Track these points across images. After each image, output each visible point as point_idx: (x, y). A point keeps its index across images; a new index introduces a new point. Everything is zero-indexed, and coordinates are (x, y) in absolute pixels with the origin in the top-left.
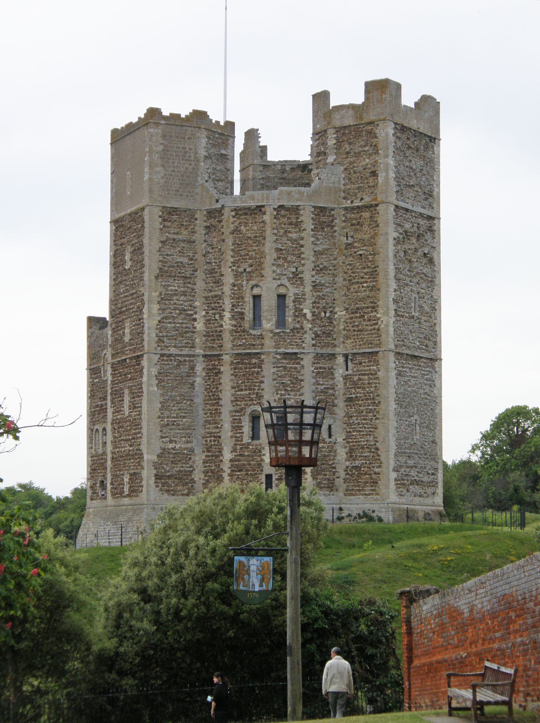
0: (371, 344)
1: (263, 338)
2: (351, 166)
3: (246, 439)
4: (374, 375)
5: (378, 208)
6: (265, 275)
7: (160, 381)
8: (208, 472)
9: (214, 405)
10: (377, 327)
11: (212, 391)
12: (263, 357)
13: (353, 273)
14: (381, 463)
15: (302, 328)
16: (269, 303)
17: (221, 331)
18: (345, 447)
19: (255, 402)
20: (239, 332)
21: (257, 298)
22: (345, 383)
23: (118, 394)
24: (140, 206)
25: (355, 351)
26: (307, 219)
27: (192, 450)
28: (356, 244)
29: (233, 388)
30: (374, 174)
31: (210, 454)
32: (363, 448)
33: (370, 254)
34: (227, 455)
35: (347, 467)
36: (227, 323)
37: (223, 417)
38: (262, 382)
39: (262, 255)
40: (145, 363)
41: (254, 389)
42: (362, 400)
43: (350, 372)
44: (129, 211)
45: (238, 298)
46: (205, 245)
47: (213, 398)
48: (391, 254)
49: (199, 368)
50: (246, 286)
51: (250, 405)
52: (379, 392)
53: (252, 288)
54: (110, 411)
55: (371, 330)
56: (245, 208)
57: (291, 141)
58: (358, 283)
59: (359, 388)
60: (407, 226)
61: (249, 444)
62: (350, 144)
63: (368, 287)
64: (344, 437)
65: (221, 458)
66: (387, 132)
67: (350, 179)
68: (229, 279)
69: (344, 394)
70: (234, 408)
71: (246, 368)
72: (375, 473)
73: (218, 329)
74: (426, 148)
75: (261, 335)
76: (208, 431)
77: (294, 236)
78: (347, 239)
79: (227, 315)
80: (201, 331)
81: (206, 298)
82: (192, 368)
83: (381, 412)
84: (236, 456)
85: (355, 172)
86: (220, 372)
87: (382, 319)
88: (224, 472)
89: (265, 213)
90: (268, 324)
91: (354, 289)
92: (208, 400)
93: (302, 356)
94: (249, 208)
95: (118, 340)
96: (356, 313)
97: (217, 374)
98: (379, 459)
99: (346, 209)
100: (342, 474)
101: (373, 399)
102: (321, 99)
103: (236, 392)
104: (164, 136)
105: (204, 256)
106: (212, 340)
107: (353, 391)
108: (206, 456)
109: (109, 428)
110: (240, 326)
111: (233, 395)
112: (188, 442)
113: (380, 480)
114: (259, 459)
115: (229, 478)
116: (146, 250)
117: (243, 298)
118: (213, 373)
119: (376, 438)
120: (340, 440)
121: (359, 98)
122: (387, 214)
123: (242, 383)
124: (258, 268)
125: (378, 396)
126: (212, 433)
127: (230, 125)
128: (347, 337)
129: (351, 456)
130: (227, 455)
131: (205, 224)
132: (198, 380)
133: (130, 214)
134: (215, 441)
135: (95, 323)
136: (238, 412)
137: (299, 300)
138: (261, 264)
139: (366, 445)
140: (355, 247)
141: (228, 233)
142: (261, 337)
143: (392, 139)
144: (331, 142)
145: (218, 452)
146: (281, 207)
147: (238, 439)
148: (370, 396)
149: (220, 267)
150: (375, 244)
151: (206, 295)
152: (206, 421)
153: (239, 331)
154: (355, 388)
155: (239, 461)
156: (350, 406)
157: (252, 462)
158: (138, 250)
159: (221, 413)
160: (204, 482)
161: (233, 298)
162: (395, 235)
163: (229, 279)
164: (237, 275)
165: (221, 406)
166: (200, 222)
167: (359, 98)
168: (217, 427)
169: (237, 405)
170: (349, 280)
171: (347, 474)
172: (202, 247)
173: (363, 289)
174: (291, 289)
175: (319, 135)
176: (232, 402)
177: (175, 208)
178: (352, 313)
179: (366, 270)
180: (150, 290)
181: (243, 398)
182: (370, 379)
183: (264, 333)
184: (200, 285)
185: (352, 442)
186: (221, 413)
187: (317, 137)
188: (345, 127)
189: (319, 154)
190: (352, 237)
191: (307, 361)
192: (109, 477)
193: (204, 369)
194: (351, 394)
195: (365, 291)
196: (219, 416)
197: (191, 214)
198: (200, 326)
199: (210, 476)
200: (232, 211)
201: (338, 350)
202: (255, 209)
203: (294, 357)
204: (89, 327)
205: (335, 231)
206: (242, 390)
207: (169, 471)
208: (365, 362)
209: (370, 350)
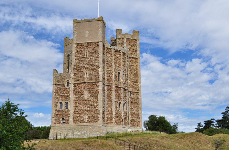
3: (118, 110)
12: (121, 88)
21: (119, 73)
24: (97, 41)
34: (114, 113)
37: (113, 102)
44: (87, 42)
45: (116, 72)
47: (110, 97)
58: (132, 75)
65: (112, 114)
68: (114, 67)
72: (139, 122)
81: (107, 70)
89: (121, 53)
97: (110, 91)
99: (129, 57)
111: (115, 97)
118: (110, 91)
128: (130, 88)
131: (107, 51)
133: (88, 43)
144: (125, 41)
147: (116, 109)
152: (107, 103)
163: (114, 67)
188: (129, 39)
191: (127, 92)
198: (106, 78)
200: (114, 50)
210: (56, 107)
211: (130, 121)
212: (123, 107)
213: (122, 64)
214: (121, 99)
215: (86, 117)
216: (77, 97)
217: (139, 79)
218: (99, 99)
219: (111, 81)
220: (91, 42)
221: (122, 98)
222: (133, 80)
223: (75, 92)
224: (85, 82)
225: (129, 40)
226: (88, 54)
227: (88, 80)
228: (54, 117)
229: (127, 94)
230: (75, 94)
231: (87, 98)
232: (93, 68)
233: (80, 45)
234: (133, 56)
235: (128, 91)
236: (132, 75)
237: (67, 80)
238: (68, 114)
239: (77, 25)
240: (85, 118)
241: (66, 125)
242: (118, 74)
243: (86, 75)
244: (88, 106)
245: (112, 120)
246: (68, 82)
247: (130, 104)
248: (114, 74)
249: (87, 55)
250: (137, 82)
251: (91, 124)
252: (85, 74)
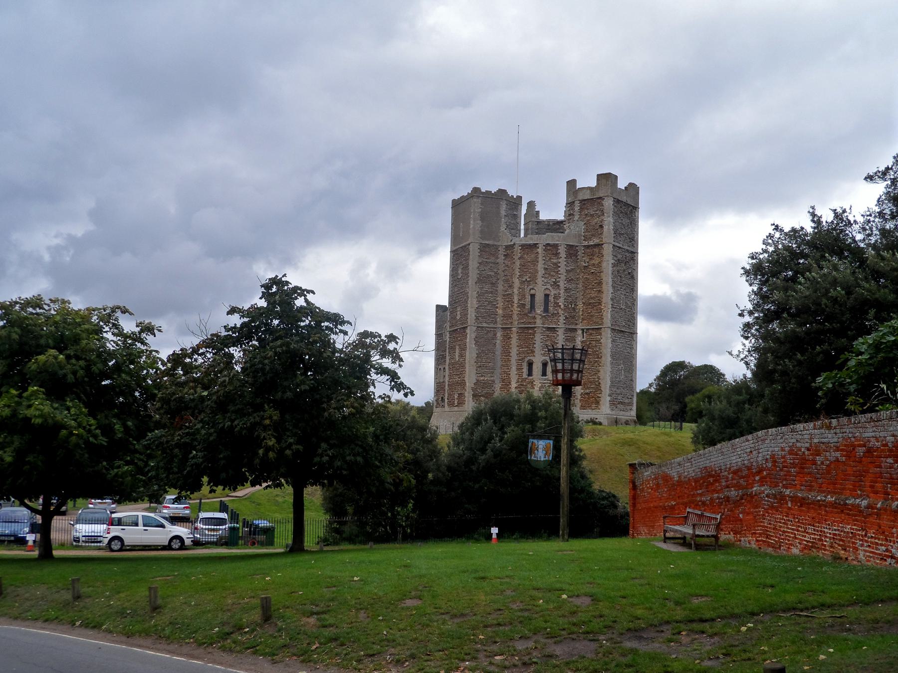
3: (525, 376)
4: (598, 341)
7: (477, 342)
16: (540, 298)
21: (533, 296)
23: (452, 348)
26: (562, 251)
30: (601, 226)
36: (516, 310)
40: (468, 331)
45: (522, 296)
47: (506, 352)
48: (610, 272)
49: (499, 335)
50: (527, 290)
54: (448, 358)
56: (527, 245)
57: (553, 209)
60: (619, 256)
66: (608, 203)
68: (517, 283)
74: (631, 212)
77: (555, 261)
79: (516, 305)
82: (495, 335)
90: (539, 310)
95: (453, 318)
100: (579, 397)
102: (571, 184)
104: (482, 204)
109: (447, 368)
116: (470, 268)
118: (507, 338)
121: (593, 184)
122: (607, 250)
124: (533, 279)
127: (520, 198)
128: (583, 319)
132: (498, 342)
135: (439, 308)
142: (534, 318)
143: (612, 207)
144: (577, 208)
146: (548, 244)
153: (522, 315)
158: (466, 267)
162: (613, 261)
163: (517, 283)
164: (522, 283)
166: (502, 251)
167: (593, 184)
172: (502, 267)
175: (570, 205)
180: (472, 291)
181: (523, 352)
184: (500, 287)
189: (570, 215)
192: (446, 395)
197: (496, 247)
201: (579, 327)
204: (437, 311)
213: (541, 272)
214: (533, 352)
219: (511, 317)
234: (596, 241)
248: (516, 301)
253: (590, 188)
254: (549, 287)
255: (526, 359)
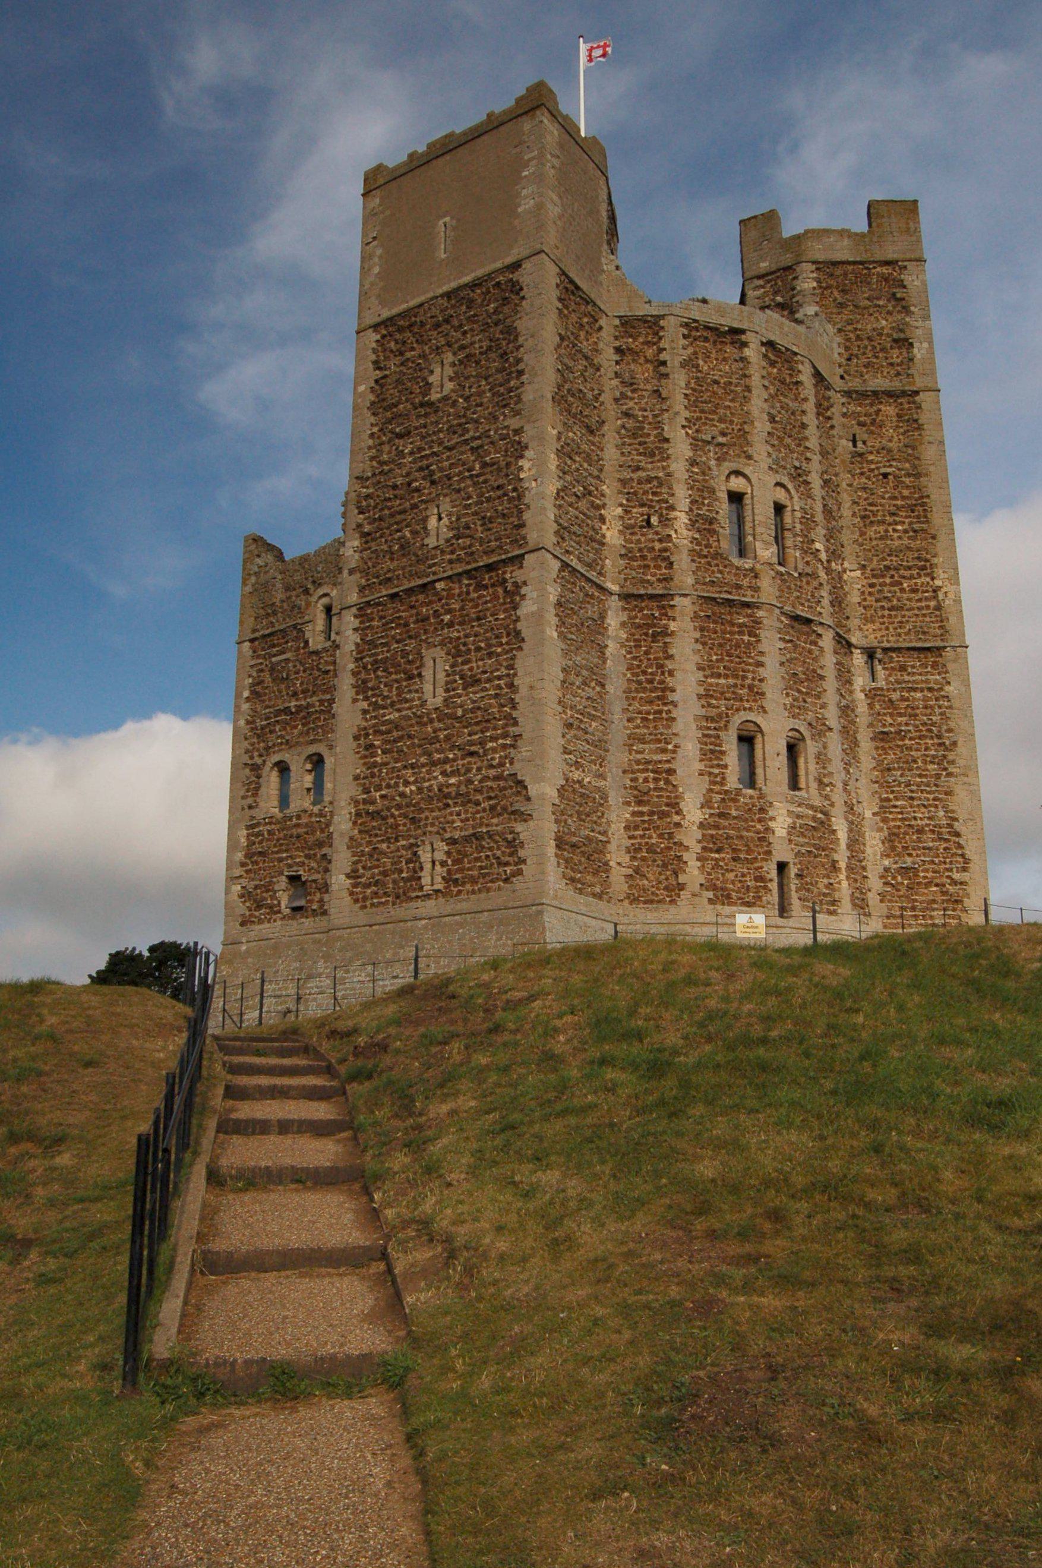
0: (924, 633)
1: (756, 577)
2: (850, 328)
3: (733, 781)
4: (937, 692)
5: (917, 398)
6: (756, 457)
8: (638, 850)
9: (651, 702)
10: (933, 604)
11: (645, 673)
12: (760, 613)
13: (871, 505)
14: (967, 861)
15: (814, 575)
17: (666, 550)
18: (880, 830)
19: (747, 706)
20: (706, 557)
22: (871, 706)
24: (509, 260)
25: (886, 645)
27: (605, 797)
28: (871, 457)
29: (700, 668)
31: (645, 809)
32: (920, 831)
33: (909, 475)
34: (693, 812)
35: (887, 870)
37: (678, 727)
38: (761, 664)
39: (747, 420)
41: (744, 678)
42: (911, 739)
43: (881, 683)
44: (445, 288)
45: (702, 491)
46: (615, 382)
47: (652, 687)
49: (614, 620)
51: (738, 710)
52: (952, 724)
53: (728, 477)
55: (919, 609)
59: (900, 715)
61: (738, 792)
62: (844, 291)
63: (906, 531)
64: (876, 810)
65: (677, 818)
67: (847, 348)
68: (681, 448)
69: (871, 725)
70: (703, 712)
71: (724, 632)
72: (954, 882)
73: (657, 546)
75: (752, 570)
76: (639, 756)
78: (855, 446)
79: (681, 518)
80: (614, 546)
81: (623, 482)
82: (602, 617)
83: (961, 762)
84: (711, 815)
85: (858, 338)
86: (665, 633)
87: (943, 590)
88: (687, 848)
89: (745, 344)
91: (876, 532)
92: (637, 691)
93: (820, 630)
94: (714, 330)
96: (883, 576)
98: (963, 856)
99: (848, 394)
101: (939, 737)
103: (706, 677)
105: (616, 400)
106: (640, 567)
107: (889, 720)
108: (634, 814)
110: (708, 546)
112: (601, 776)
113: (968, 896)
114: (759, 826)
115: (699, 864)
117: (713, 491)
119: (953, 811)
120: (868, 814)
121: (861, 225)
123: (717, 661)
125: (950, 730)
126: (649, 762)
128: (867, 620)
129: (893, 848)
130: (693, 812)
131: (617, 344)
132: (612, 647)
133: (448, 295)
134: (656, 780)
136: (711, 719)
137: (808, 521)
138: (743, 434)
139: (928, 825)
140: (872, 462)
141: (677, 364)
145: (667, 805)
148: (930, 731)
149: (658, 425)
150: (918, 459)
151: (627, 475)
153: (706, 555)
154: (891, 715)
155: (717, 827)
156: (883, 748)
157: (745, 833)
159: (674, 719)
160: (630, 871)
161: (692, 488)
163: (681, 448)
164: (697, 444)
165: (674, 704)
168: (664, 751)
169: (709, 705)
170: (863, 517)
171: (886, 884)
173: (896, 535)
174: (796, 499)
176: (699, 697)
177: (578, 288)
178: (874, 576)
179: (899, 503)
182: (926, 699)
183: (758, 566)
184: (611, 454)
185: (894, 820)
186: (674, 719)
187: (761, 282)
188: (835, 264)
190: (864, 443)
191: (827, 641)
193: (623, 624)
194: (884, 726)
195: (900, 538)
196: (669, 727)
198: (612, 535)
199: (643, 859)
202: (726, 333)
203: (805, 628)
205: (832, 427)
206: (719, 676)
207: (574, 834)
208: (913, 667)
209: (920, 645)
210: (250, 801)
211: (875, 884)
212: (783, 758)
213: (761, 427)
215: (433, 853)
216: (376, 706)
217: (941, 545)
218: (523, 691)
220: (467, 279)
221: (765, 687)
222: (894, 561)
223: (365, 668)
224: (432, 578)
225: (838, 271)
226: (449, 371)
227: (451, 562)
228: (238, 871)
229: (829, 660)
230: (364, 682)
231: (439, 701)
232: (484, 465)
233: (401, 330)
234: (878, 382)
235: (844, 645)
236: (883, 522)
237: (320, 592)
238: (320, 844)
239: (382, 198)
240: (425, 856)
241: (308, 923)
242: (724, 509)
243: (438, 527)
244: (446, 761)
245: (676, 865)
246: (328, 609)
247: (866, 745)
249: (441, 379)
250: (927, 568)
251: (464, 906)
252: (433, 522)
253: (843, 233)
254: (785, 480)
255: (737, 719)
